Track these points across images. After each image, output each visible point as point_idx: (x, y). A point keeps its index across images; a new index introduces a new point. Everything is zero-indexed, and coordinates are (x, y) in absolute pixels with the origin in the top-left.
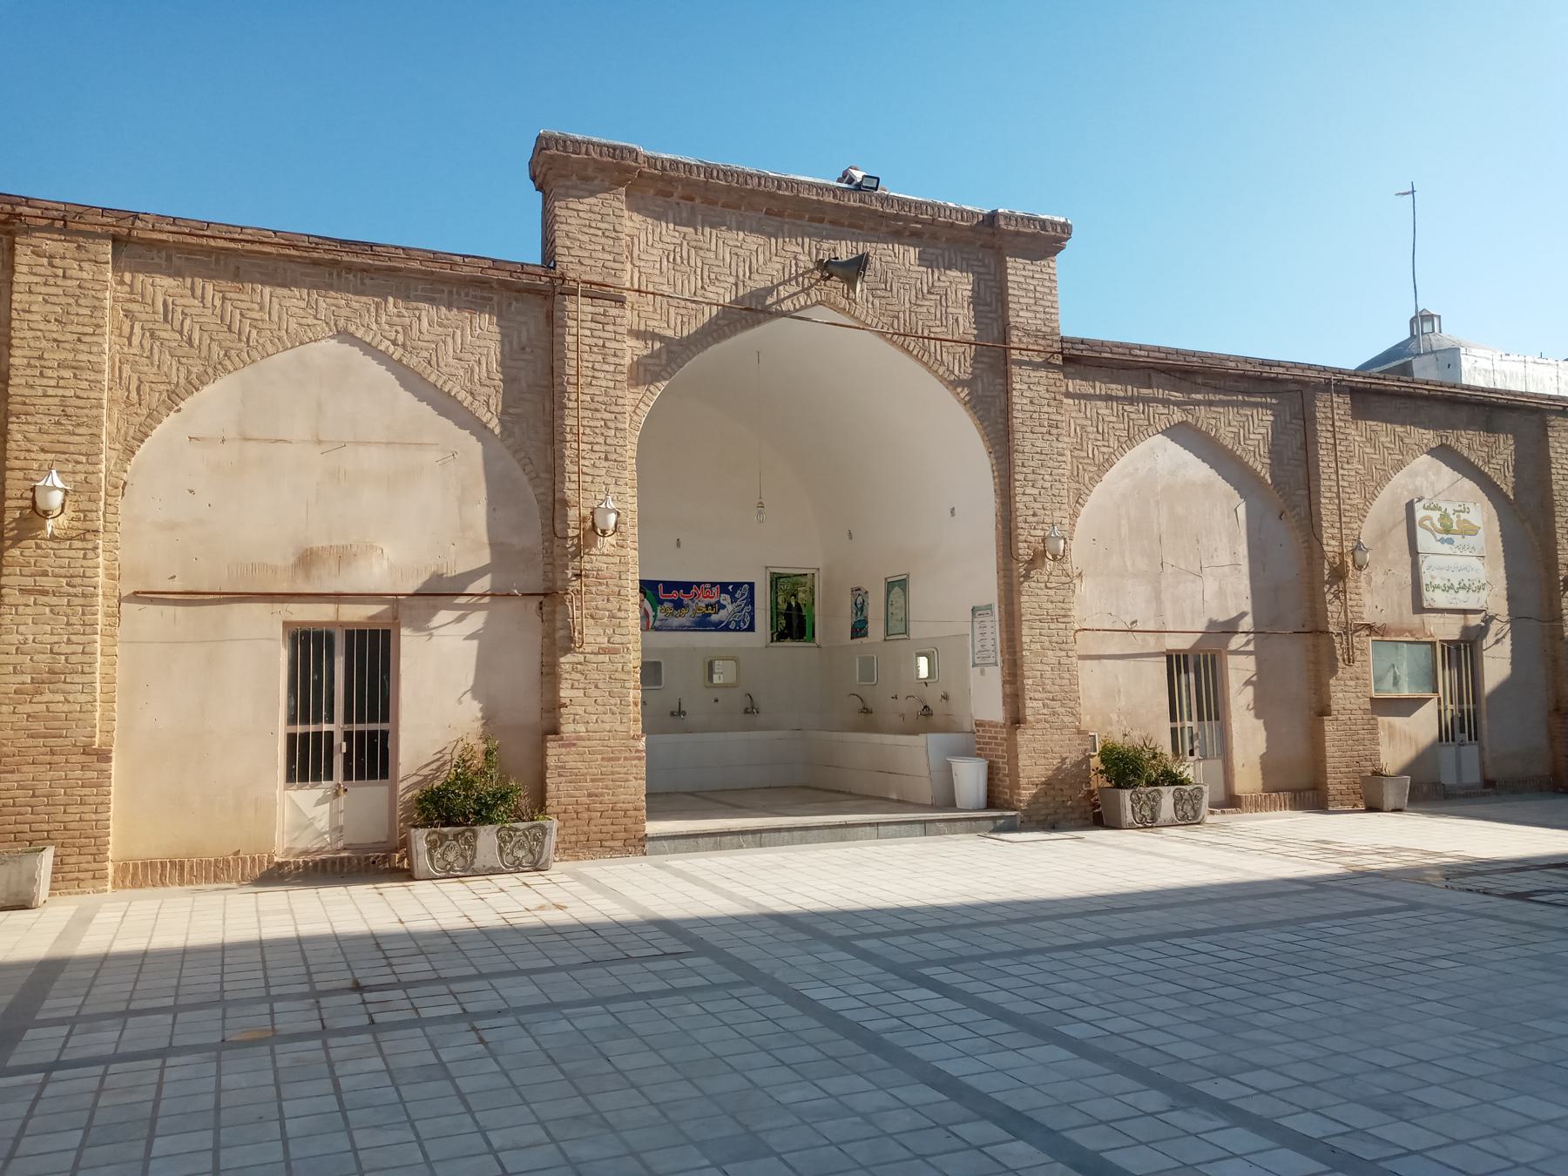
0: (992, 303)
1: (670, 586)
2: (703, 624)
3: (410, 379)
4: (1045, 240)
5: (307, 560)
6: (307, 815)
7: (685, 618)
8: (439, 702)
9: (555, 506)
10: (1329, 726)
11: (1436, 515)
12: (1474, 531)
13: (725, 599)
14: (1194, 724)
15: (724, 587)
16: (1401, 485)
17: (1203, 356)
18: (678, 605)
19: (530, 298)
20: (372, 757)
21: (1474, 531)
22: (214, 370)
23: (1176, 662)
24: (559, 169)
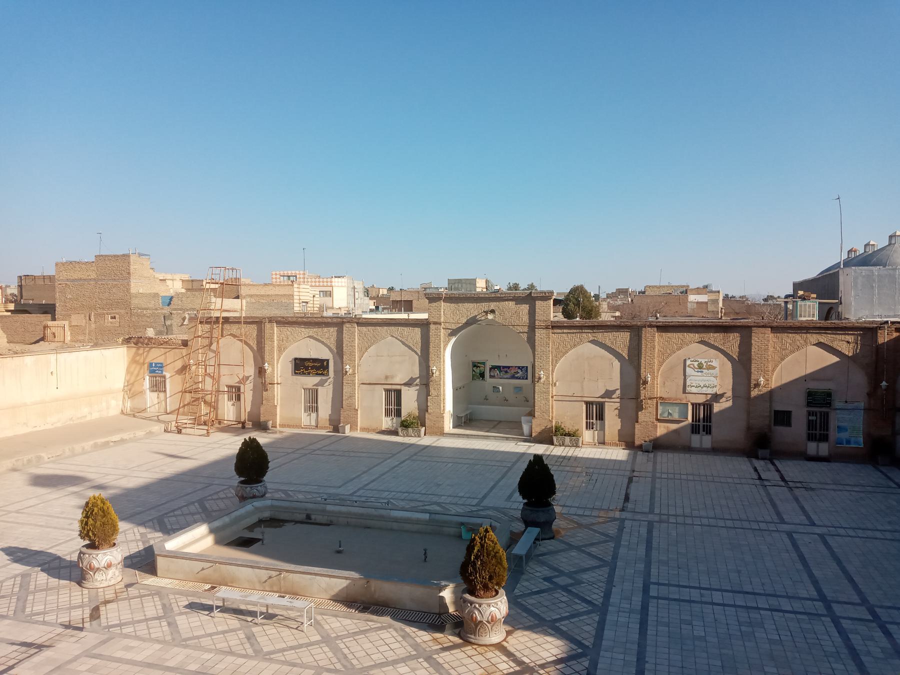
0: (532, 313)
1: (504, 367)
2: (513, 377)
3: (403, 343)
5: (387, 377)
6: (387, 423)
7: (508, 375)
8: (410, 402)
9: (428, 367)
10: (637, 426)
11: (696, 364)
12: (714, 368)
13: (519, 371)
14: (594, 421)
15: (519, 367)
16: (682, 354)
18: (506, 372)
20: (398, 413)
21: (714, 368)
22: (372, 344)
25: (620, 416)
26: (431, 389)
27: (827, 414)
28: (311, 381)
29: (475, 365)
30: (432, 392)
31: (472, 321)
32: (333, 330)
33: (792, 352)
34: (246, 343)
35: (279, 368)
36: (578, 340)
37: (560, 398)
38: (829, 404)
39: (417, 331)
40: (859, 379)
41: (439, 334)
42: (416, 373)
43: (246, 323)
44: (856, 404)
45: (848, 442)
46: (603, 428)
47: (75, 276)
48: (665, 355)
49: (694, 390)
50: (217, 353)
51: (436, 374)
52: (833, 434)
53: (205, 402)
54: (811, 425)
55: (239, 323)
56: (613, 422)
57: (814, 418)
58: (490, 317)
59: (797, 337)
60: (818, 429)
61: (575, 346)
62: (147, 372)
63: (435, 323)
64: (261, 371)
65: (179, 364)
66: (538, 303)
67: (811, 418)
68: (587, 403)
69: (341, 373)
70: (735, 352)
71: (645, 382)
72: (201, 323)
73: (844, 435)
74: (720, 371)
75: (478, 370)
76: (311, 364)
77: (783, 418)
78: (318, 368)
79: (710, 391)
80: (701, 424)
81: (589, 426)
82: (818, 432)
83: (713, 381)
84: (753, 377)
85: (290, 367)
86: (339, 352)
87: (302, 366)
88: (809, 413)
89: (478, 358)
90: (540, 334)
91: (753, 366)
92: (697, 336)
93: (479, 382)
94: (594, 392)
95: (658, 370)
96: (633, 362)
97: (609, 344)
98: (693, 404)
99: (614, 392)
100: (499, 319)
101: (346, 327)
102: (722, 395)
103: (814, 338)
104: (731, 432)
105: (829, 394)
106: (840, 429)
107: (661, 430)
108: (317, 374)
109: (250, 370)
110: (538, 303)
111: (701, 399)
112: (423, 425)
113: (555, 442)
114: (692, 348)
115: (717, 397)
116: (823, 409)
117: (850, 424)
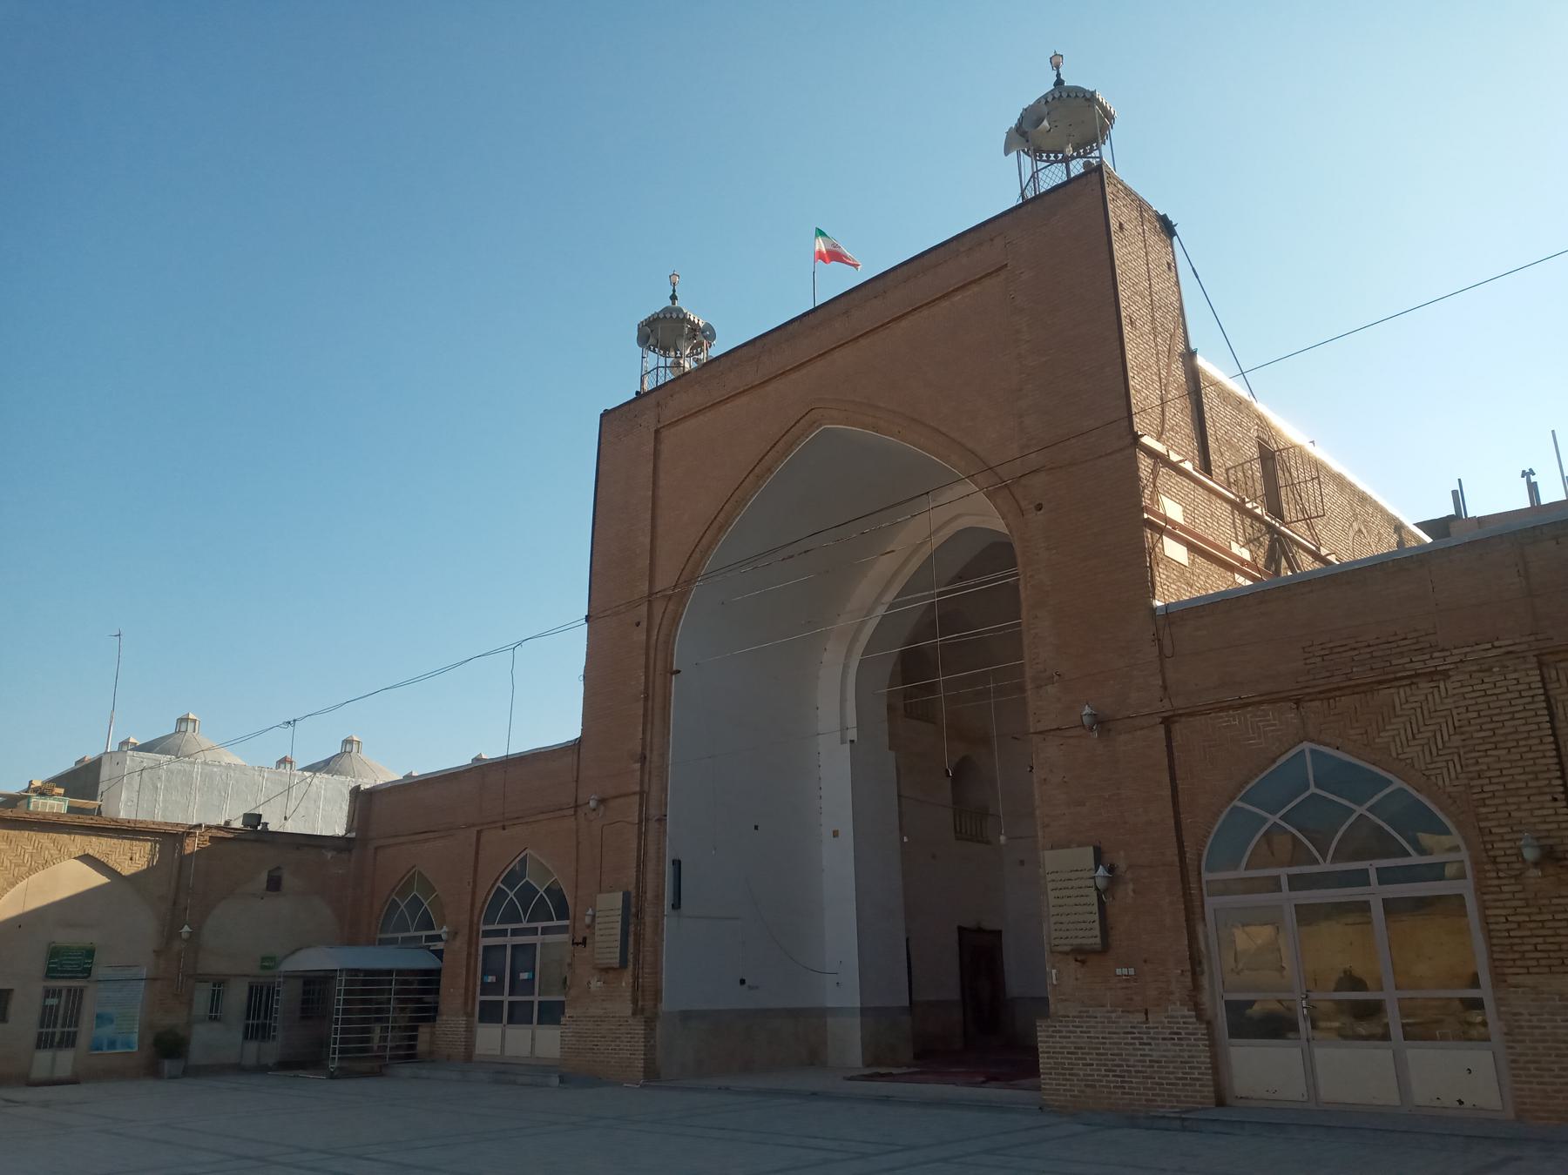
33: (32, 871)
38: (87, 972)
45: (112, 1044)
52: (87, 1030)
54: (48, 1017)
57: (52, 1001)
60: (57, 1030)
73: (107, 1031)
88: (48, 993)
105: (90, 953)
106: (101, 1019)
117: (120, 1010)
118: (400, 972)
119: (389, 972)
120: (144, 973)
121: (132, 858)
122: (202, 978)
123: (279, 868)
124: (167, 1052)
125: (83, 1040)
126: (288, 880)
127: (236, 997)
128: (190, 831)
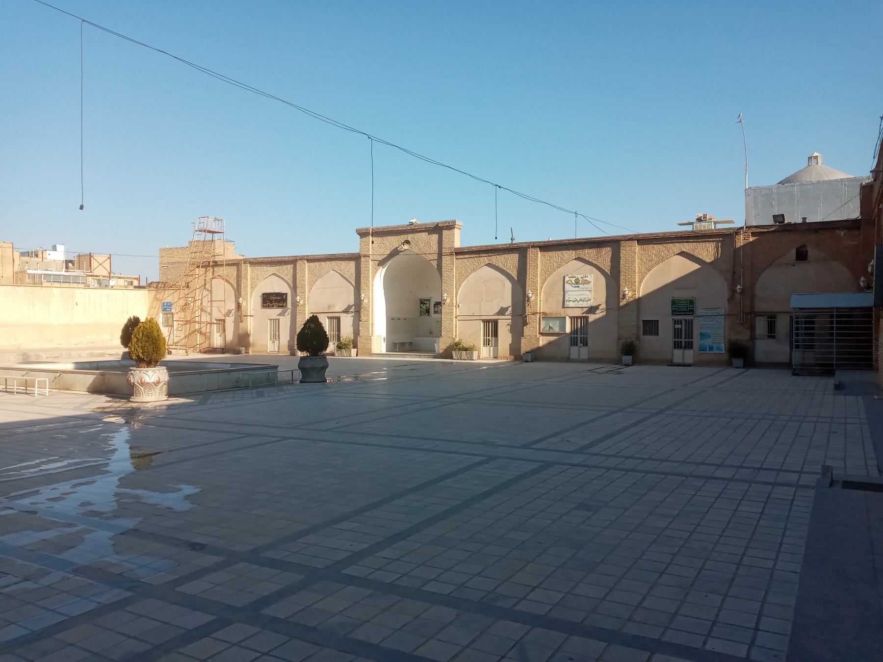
4: (451, 226)
5: (329, 307)
10: (523, 340)
11: (573, 279)
12: (589, 282)
16: (561, 271)
17: (492, 246)
19: (356, 258)
21: (589, 282)
22: (319, 278)
23: (486, 322)
24: (363, 234)
25: (511, 331)
26: (362, 315)
27: (692, 322)
28: (274, 312)
29: (422, 302)
30: (363, 317)
31: (395, 253)
32: (290, 267)
33: (657, 263)
34: (227, 281)
35: (252, 303)
36: (476, 264)
37: (462, 318)
38: (692, 312)
39: (352, 264)
40: (721, 286)
41: (369, 265)
42: (352, 301)
43: (227, 265)
44: (718, 310)
45: (711, 348)
46: (496, 345)
47: (174, 260)
48: (547, 273)
49: (571, 304)
50: (211, 292)
51: (366, 301)
53: (201, 333)
54: (677, 333)
55: (222, 265)
56: (505, 337)
57: (679, 326)
58: (406, 247)
59: (660, 246)
61: (474, 270)
62: (161, 310)
63: (365, 256)
64: (239, 306)
65: (182, 302)
66: (445, 232)
67: (677, 326)
68: (485, 321)
69: (295, 304)
70: (607, 266)
71: (529, 298)
72: (198, 267)
73: (707, 342)
74: (594, 285)
75: (424, 307)
76: (274, 298)
77: (651, 327)
78: (279, 301)
79: (585, 304)
80: (579, 336)
81: (487, 343)
82: (683, 340)
83: (588, 295)
84: (621, 289)
85: (259, 301)
86: (294, 288)
87: (271, 300)
88: (676, 322)
89: (424, 296)
90: (446, 260)
91: (622, 278)
92: (572, 254)
93: (425, 318)
94: (490, 311)
95: (541, 288)
96: (520, 283)
97: (501, 266)
98: (571, 318)
99: (507, 309)
100: (415, 250)
101: (299, 263)
102: (597, 308)
103: (678, 247)
104: (607, 343)
105: (691, 302)
107: (543, 341)
108: (279, 306)
109: (232, 306)
110: (445, 232)
111: (578, 313)
112: (355, 346)
113: (454, 357)
114: (571, 265)
115: (592, 310)
116: (687, 317)
117: (713, 331)
118: (837, 308)
119: (832, 308)
120: (723, 311)
121: (707, 252)
122: (761, 314)
123: (804, 246)
124: (740, 354)
125: (696, 345)
126: (811, 252)
127: (782, 325)
128: (737, 232)
